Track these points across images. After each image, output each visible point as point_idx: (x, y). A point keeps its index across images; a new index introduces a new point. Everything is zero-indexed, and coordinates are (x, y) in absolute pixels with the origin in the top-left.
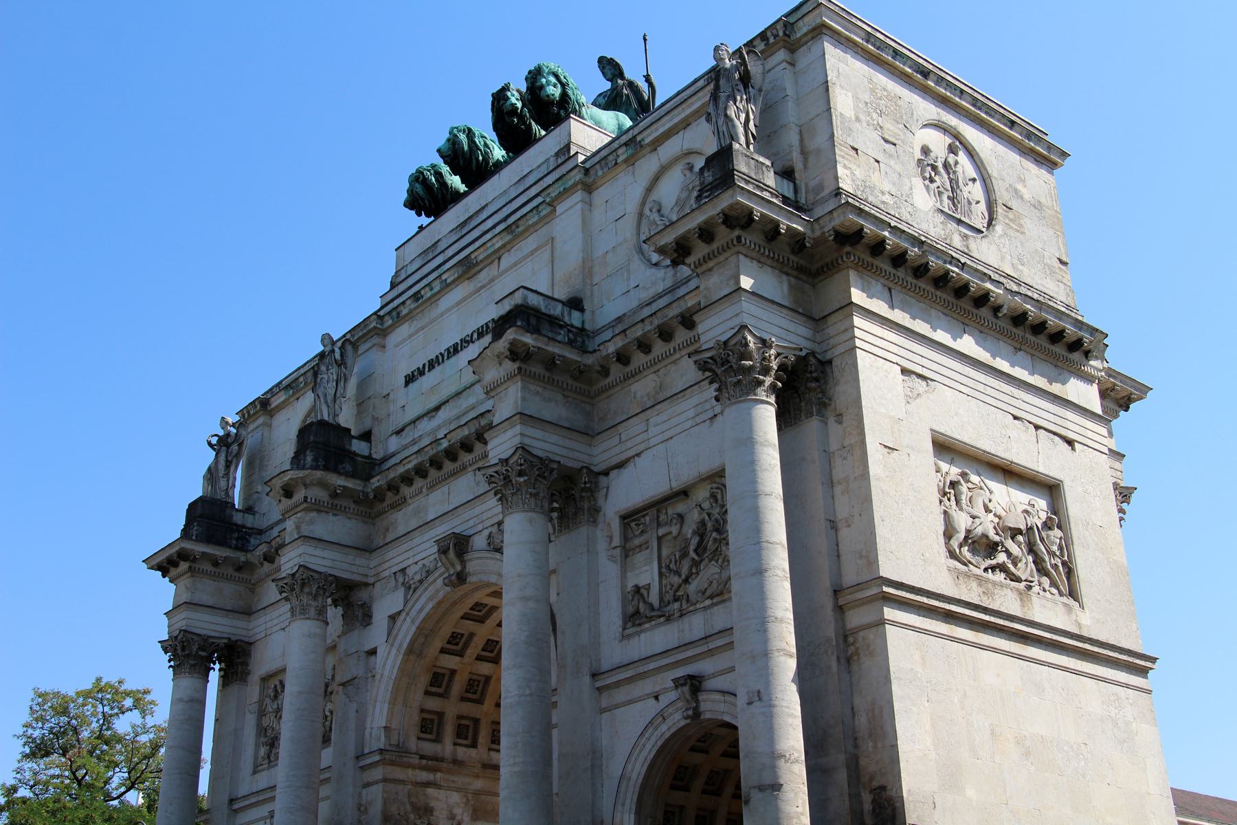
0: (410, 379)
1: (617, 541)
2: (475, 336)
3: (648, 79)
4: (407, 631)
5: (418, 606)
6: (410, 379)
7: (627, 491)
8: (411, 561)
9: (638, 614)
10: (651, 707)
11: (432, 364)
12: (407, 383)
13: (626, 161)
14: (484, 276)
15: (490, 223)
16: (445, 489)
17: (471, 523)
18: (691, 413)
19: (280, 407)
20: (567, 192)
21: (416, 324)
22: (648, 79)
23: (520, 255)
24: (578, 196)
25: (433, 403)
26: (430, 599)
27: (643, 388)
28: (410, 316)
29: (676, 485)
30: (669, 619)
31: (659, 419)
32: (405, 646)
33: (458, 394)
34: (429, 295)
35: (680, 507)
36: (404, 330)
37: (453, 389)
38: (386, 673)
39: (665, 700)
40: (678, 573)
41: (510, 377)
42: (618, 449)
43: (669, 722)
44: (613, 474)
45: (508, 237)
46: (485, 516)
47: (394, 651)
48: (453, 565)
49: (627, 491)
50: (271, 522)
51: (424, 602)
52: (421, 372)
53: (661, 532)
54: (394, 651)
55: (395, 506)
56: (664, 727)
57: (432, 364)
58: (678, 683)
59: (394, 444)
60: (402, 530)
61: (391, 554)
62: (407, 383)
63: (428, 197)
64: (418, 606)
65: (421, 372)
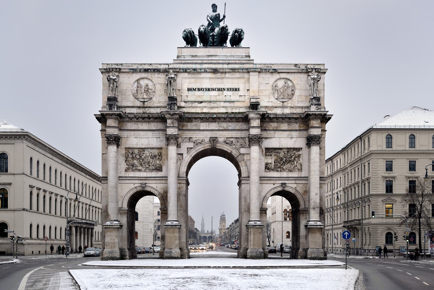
0: (189, 90)
1: (264, 153)
2: (217, 89)
3: (224, 17)
4: (193, 153)
5: (198, 148)
6: (189, 90)
7: (267, 144)
8: (194, 137)
9: (267, 168)
10: (272, 186)
11: (199, 90)
12: (188, 90)
13: (271, 72)
14: (219, 75)
15: (221, 62)
16: (207, 124)
17: (218, 135)
18: (287, 135)
19: (123, 72)
20: (255, 71)
21: (190, 76)
22: (224, 17)
23: (233, 76)
24: (257, 74)
25: (201, 100)
26: (203, 148)
27: (274, 125)
28: (189, 72)
29: (281, 147)
30: (277, 171)
31: (278, 133)
32: (193, 156)
33: (210, 102)
34: (199, 71)
35: (279, 151)
36: (186, 75)
37: (208, 99)
38: (186, 160)
39: (276, 185)
40: (280, 164)
41: (258, 119)
42: (266, 135)
43: (277, 189)
44: (263, 139)
45: (231, 71)
46: (223, 135)
47: (189, 156)
48: (214, 143)
49: (267, 144)
50: (123, 105)
51: (200, 148)
52: (195, 90)
53: (275, 154)
54: (189, 156)
55: (188, 122)
56: (276, 190)
57: (199, 90)
58: (282, 184)
59: (183, 104)
60: (189, 128)
61: (186, 133)
62: (188, 90)
63: (190, 39)
64: (198, 148)
65: (195, 90)
